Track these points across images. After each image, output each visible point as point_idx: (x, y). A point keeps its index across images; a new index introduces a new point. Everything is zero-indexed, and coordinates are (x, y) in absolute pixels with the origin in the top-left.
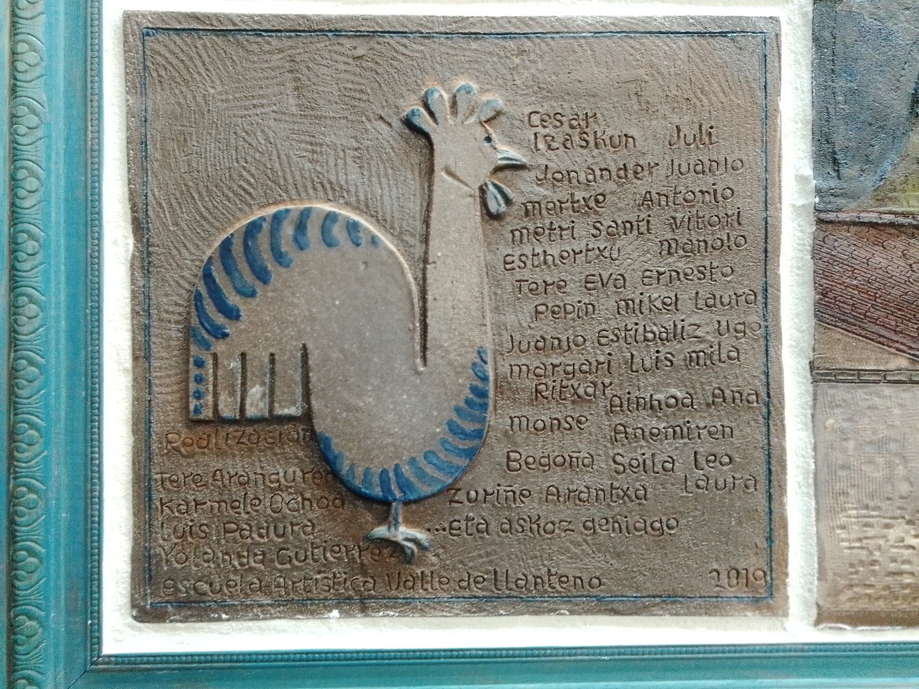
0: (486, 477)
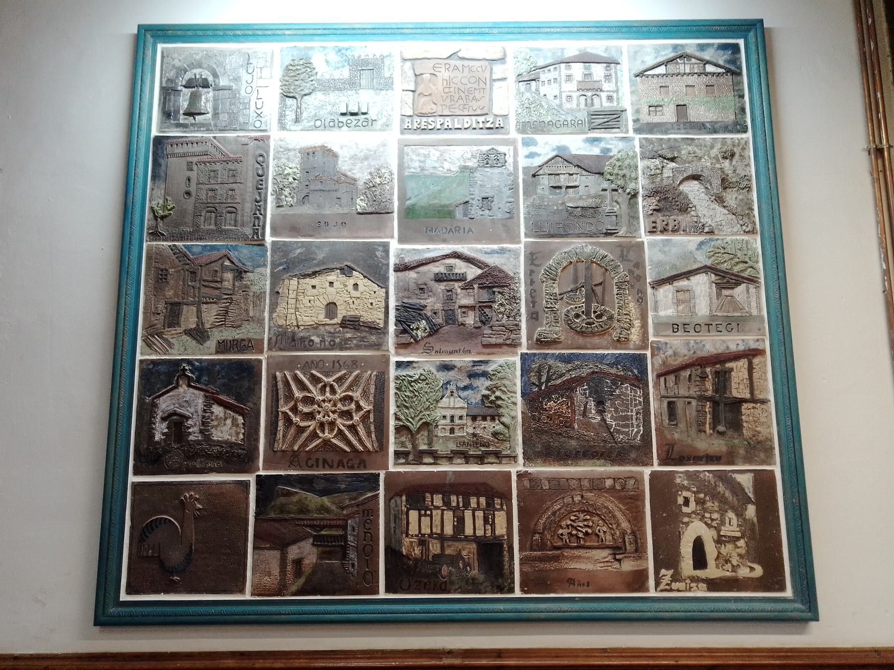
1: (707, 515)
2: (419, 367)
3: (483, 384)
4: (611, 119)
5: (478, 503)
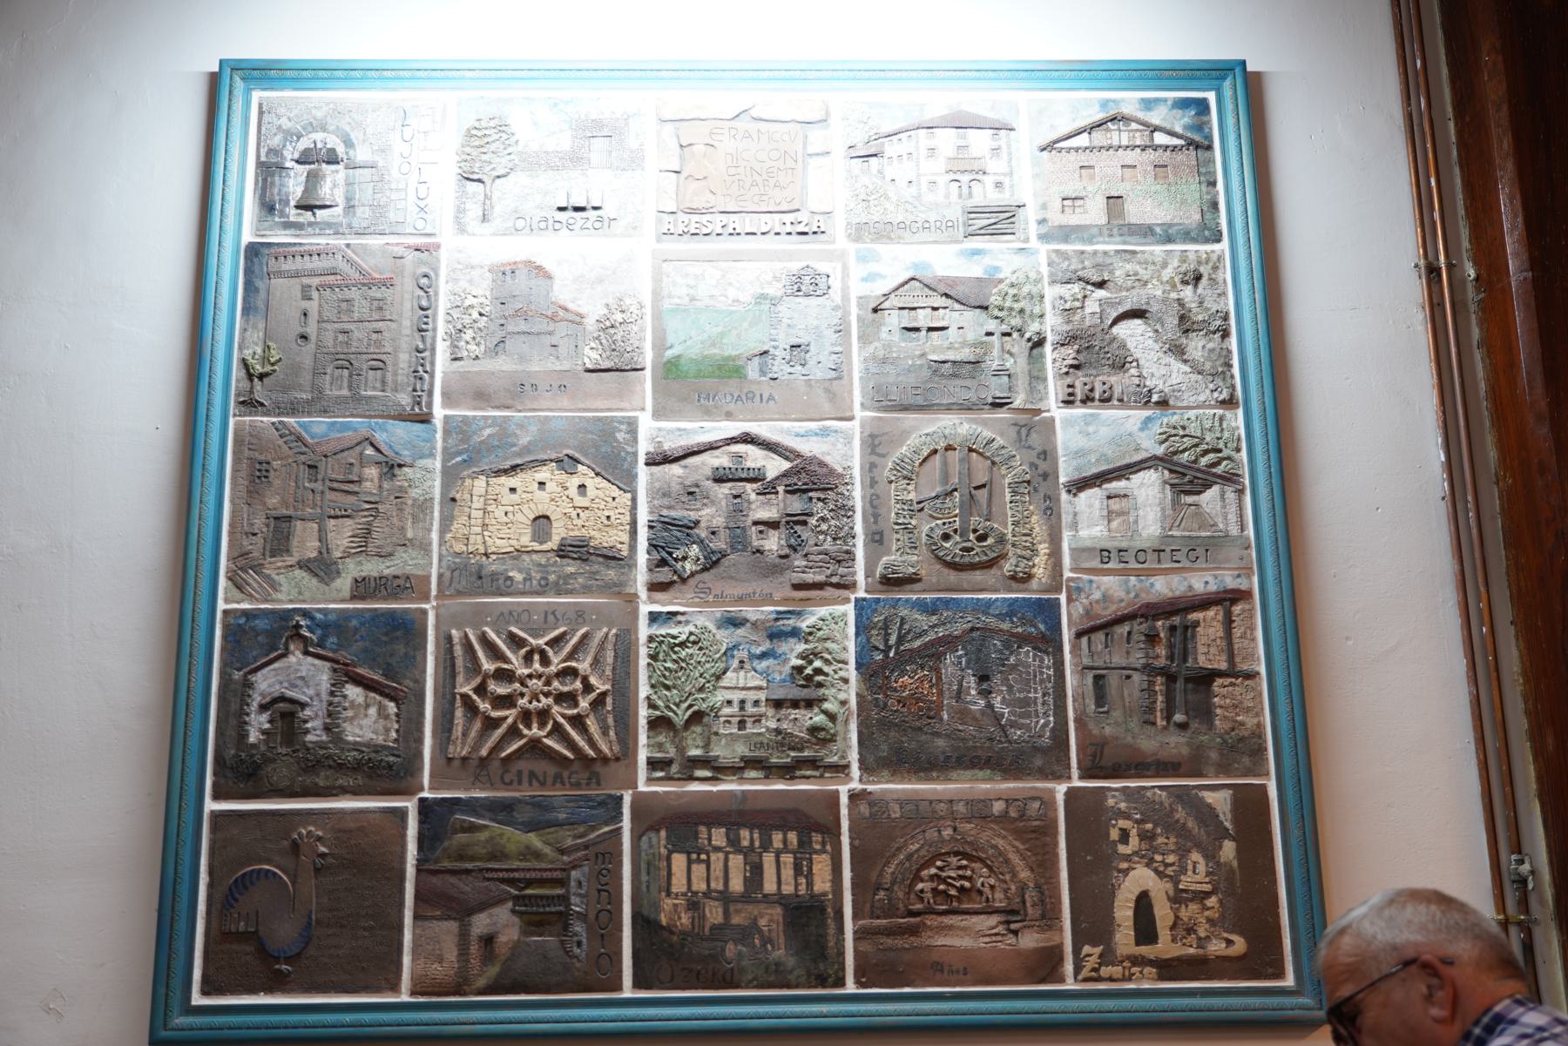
0: (311, 951)
1: (1158, 858)
2: (687, 622)
3: (793, 651)
4: (998, 221)
5: (785, 841)
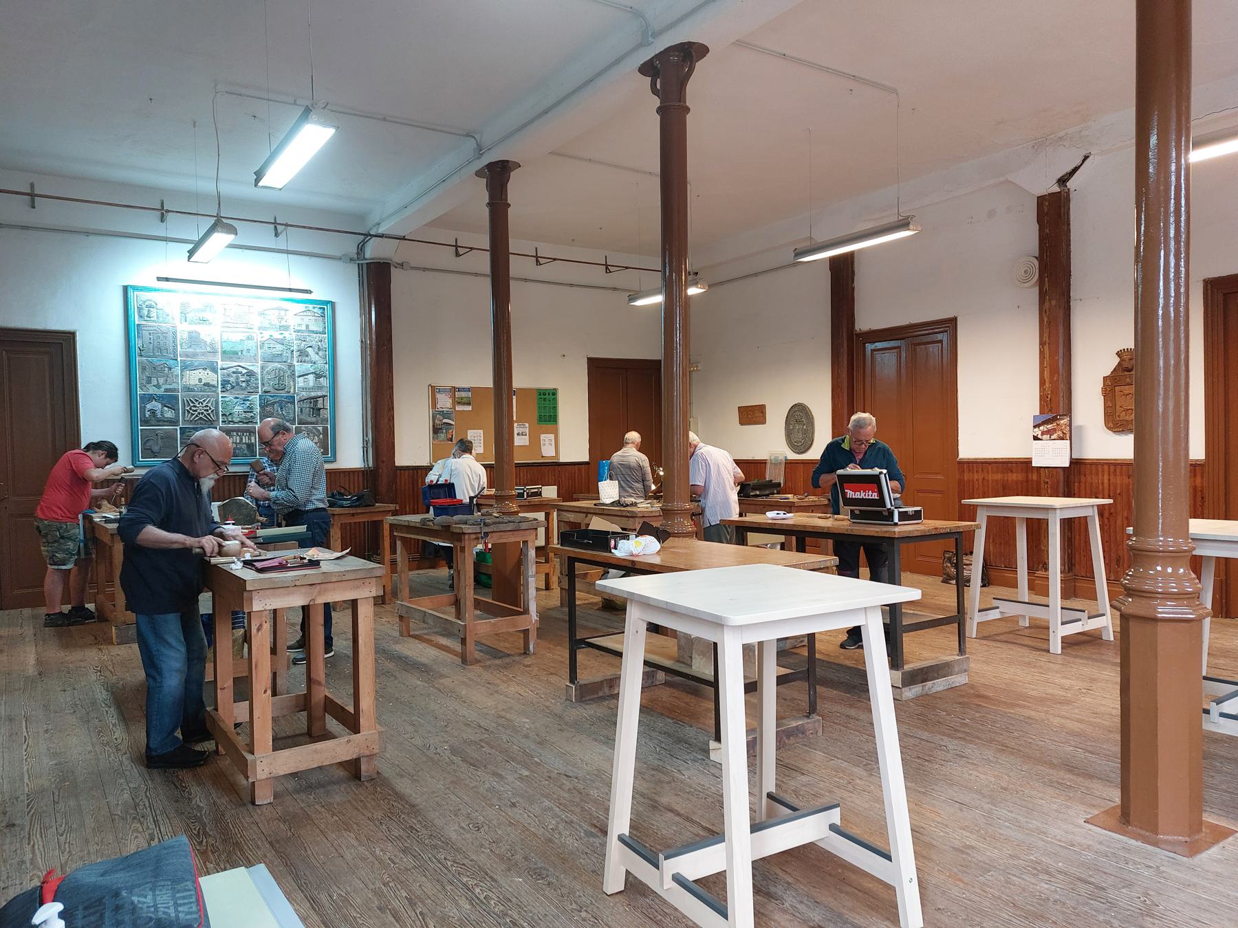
4: (286, 328)
